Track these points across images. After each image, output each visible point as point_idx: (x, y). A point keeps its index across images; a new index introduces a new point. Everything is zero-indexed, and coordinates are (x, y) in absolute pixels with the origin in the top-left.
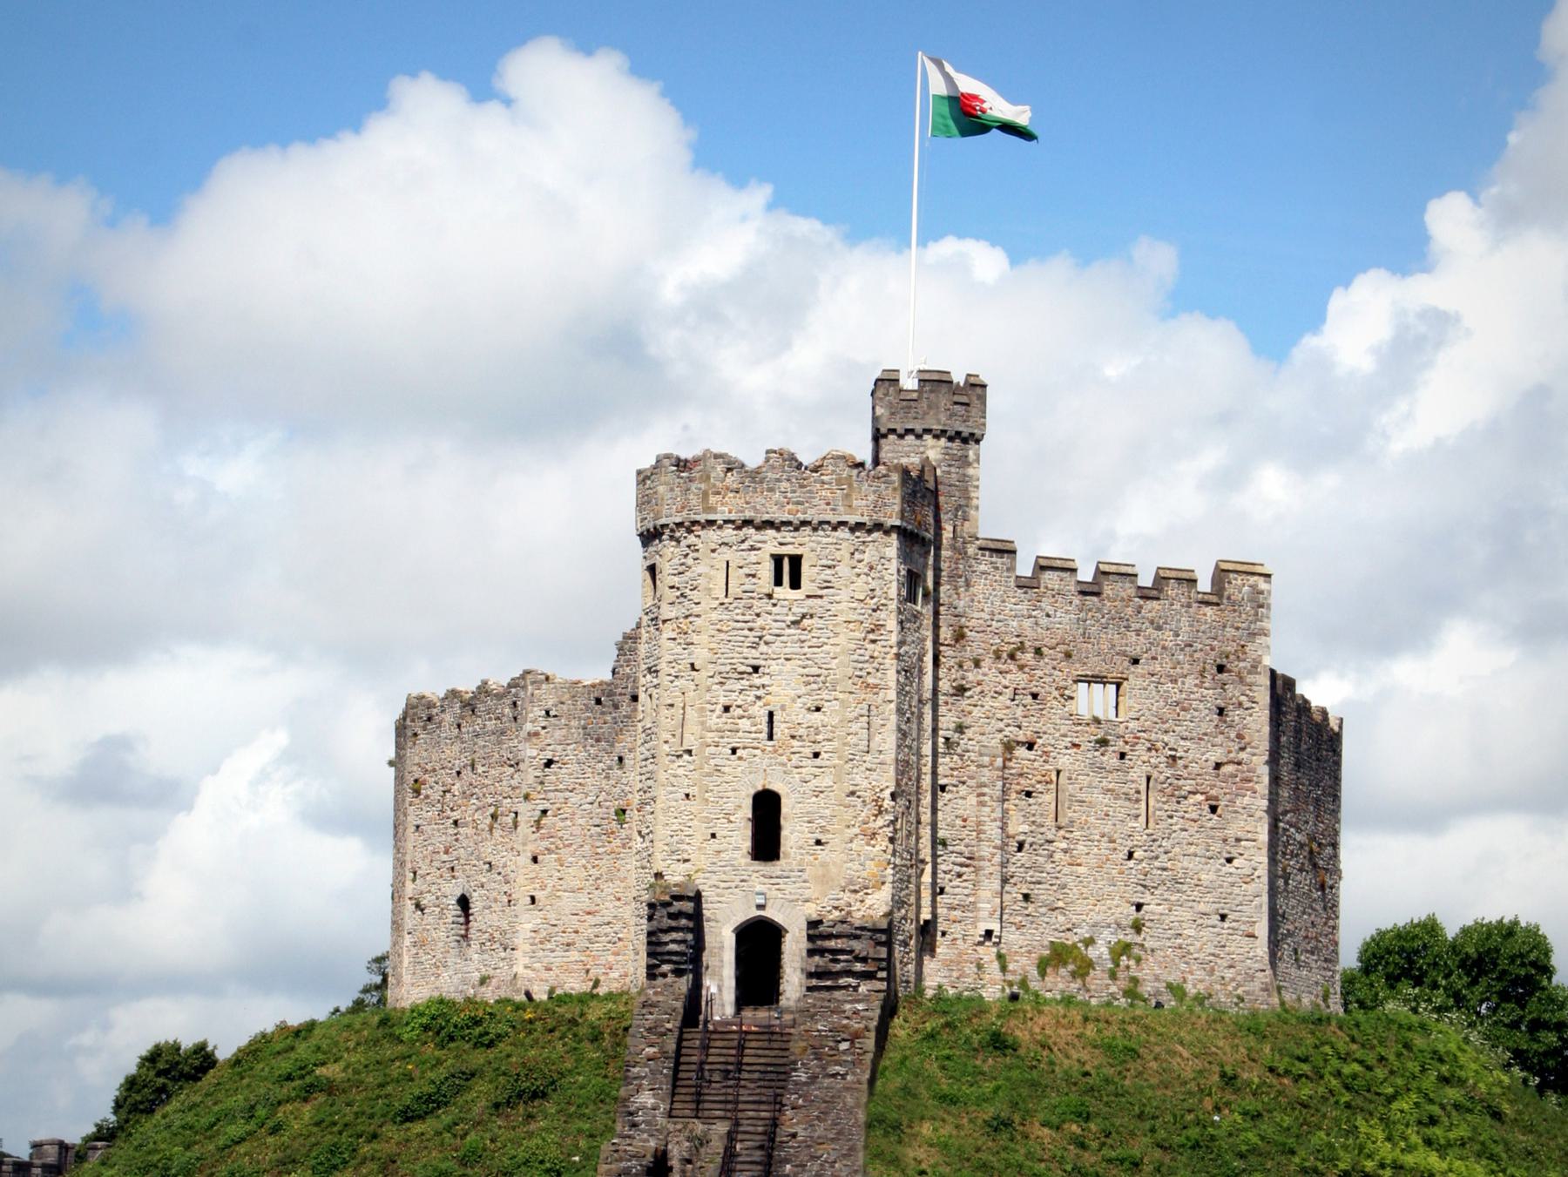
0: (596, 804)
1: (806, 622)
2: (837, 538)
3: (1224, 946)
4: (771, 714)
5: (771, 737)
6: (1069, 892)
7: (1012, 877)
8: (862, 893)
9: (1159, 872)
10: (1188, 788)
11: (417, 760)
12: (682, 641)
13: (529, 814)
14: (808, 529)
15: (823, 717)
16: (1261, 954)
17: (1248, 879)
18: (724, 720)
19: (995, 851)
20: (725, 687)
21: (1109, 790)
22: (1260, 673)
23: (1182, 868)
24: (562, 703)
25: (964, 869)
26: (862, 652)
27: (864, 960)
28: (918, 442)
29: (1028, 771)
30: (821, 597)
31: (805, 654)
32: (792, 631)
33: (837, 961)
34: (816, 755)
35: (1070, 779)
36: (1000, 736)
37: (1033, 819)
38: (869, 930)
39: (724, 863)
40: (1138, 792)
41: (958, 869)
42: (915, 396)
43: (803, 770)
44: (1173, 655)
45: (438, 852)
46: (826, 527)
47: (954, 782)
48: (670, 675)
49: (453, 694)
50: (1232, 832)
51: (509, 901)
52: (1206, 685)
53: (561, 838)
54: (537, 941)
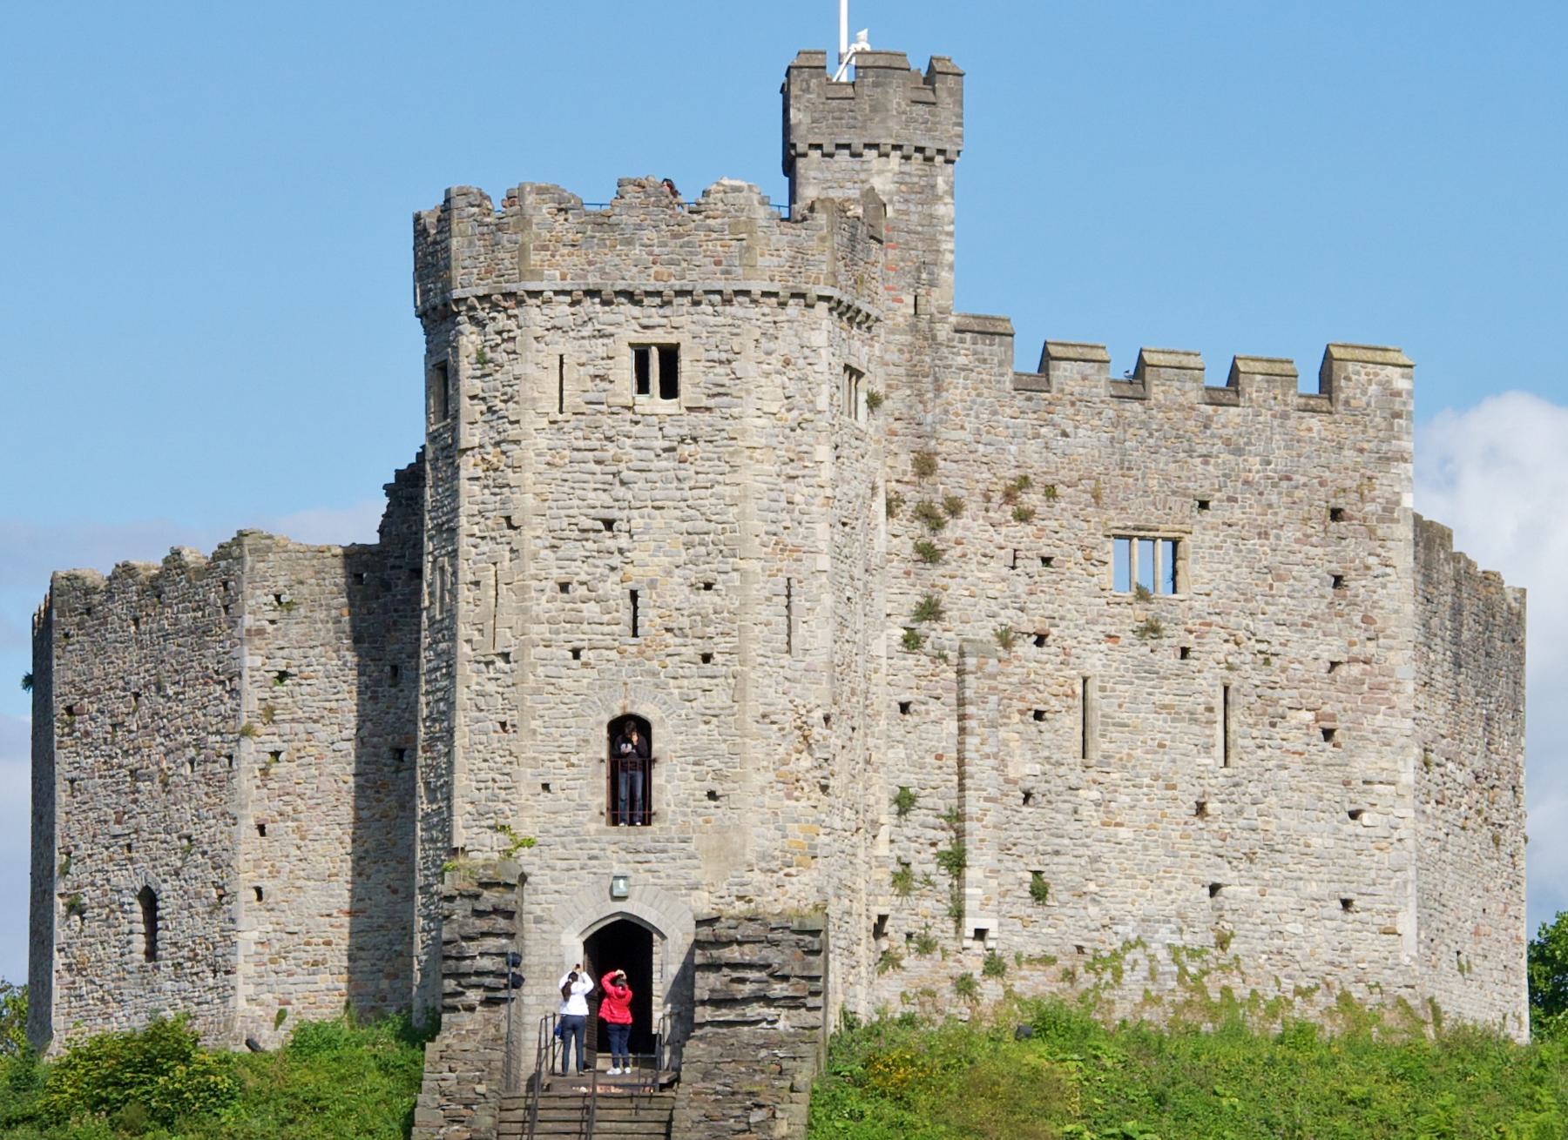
1: (685, 450)
2: (734, 317)
3: (1349, 950)
4: (634, 596)
5: (635, 635)
6: (1105, 867)
7: (1015, 845)
8: (781, 874)
9: (1245, 834)
10: (1286, 702)
11: (69, 676)
12: (491, 482)
13: (251, 759)
14: (686, 300)
15: (717, 599)
16: (1407, 960)
17: (1385, 842)
18: (558, 604)
19: (988, 805)
20: (560, 554)
21: (1165, 707)
22: (1398, 521)
23: (1281, 828)
24: (301, 583)
25: (940, 834)
26: (774, 495)
27: (785, 978)
28: (855, 164)
29: (1038, 679)
30: (708, 409)
32: (664, 464)
33: (742, 981)
34: (706, 658)
35: (1103, 689)
36: (993, 623)
37: (1046, 753)
38: (794, 932)
39: (562, 831)
40: (1210, 709)
41: (931, 834)
42: (849, 92)
43: (685, 682)
44: (1261, 494)
45: (106, 822)
46: (717, 298)
47: (922, 698)
48: (473, 535)
49: (126, 571)
50: (1361, 767)
51: (221, 897)
52: (1314, 540)
54: (266, 958)
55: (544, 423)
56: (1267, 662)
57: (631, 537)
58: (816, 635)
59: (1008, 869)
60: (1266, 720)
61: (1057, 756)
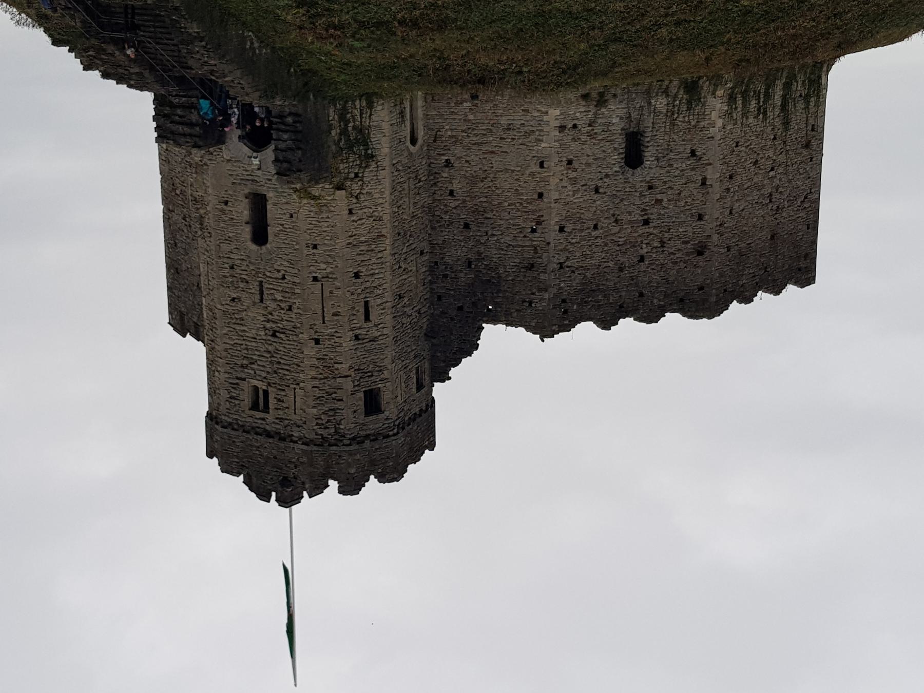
0: (490, 233)
1: (245, 362)
30: (237, 378)
31: (244, 340)
53: (518, 210)
54: (537, 133)
55: (302, 385)
57: (264, 327)
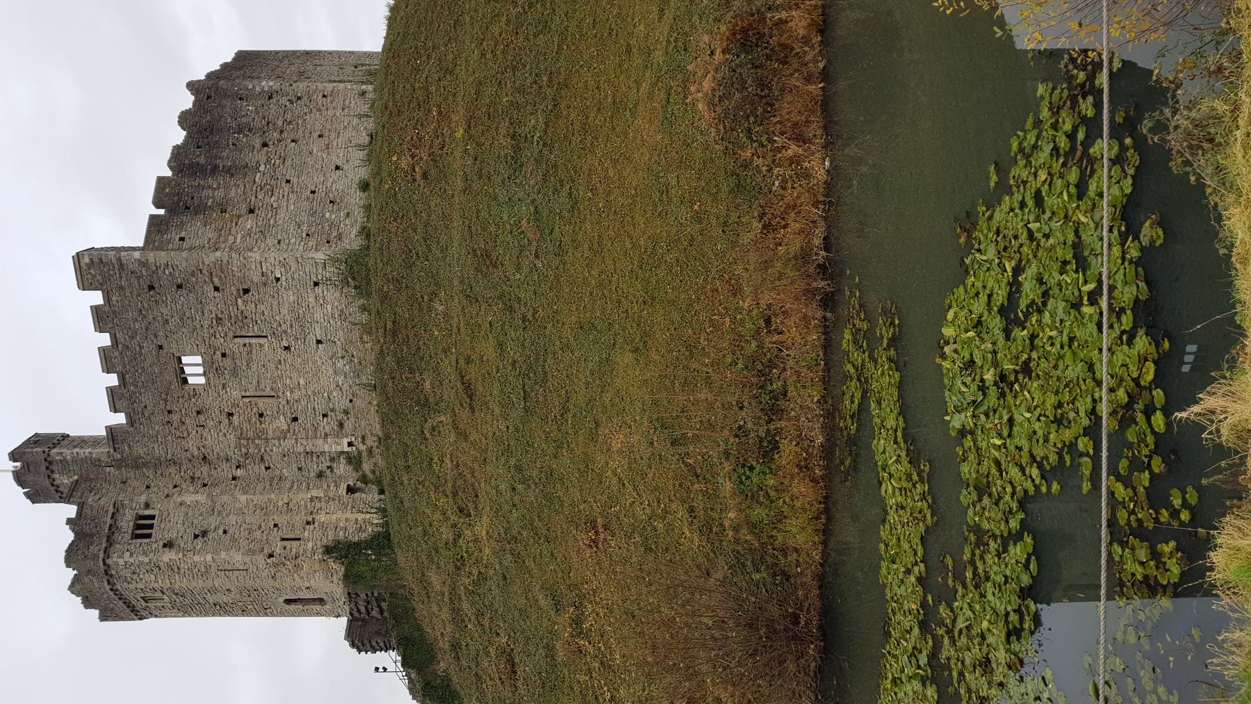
35: (246, 391)
40: (245, 345)
41: (315, 459)
56: (221, 319)
58: (238, 558)
59: (324, 429)
60: (245, 321)
61: (276, 409)
